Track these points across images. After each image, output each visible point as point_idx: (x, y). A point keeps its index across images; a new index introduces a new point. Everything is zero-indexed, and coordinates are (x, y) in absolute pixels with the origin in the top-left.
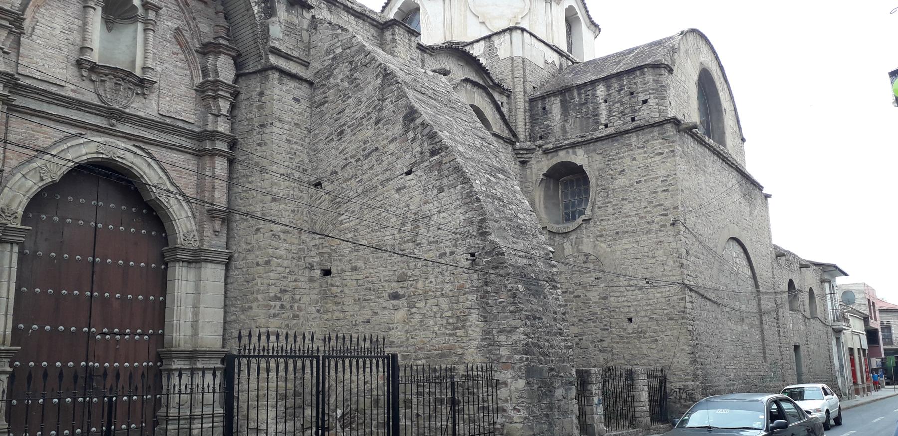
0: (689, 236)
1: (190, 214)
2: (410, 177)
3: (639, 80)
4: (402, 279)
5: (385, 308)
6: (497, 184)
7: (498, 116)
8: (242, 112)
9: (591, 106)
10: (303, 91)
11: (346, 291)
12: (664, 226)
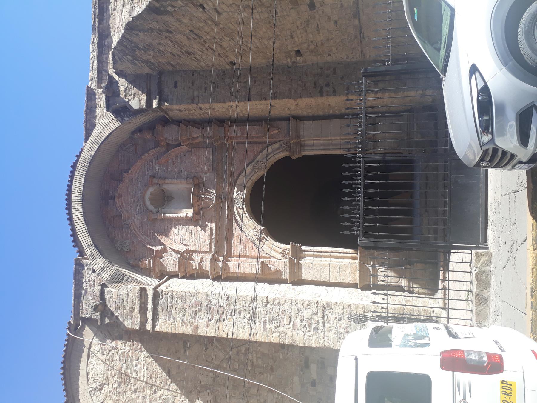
2: (205, 6)
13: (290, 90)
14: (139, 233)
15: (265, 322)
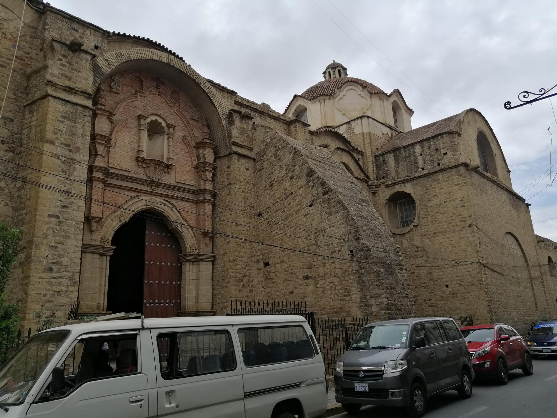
0: (480, 233)
1: (193, 235)
2: (311, 208)
3: (440, 141)
4: (310, 267)
5: (301, 285)
6: (362, 209)
7: (357, 167)
8: (219, 177)
9: (412, 158)
10: (250, 164)
11: (278, 275)
12: (464, 227)
13: (242, 257)
14: (128, 101)
15: (58, 217)
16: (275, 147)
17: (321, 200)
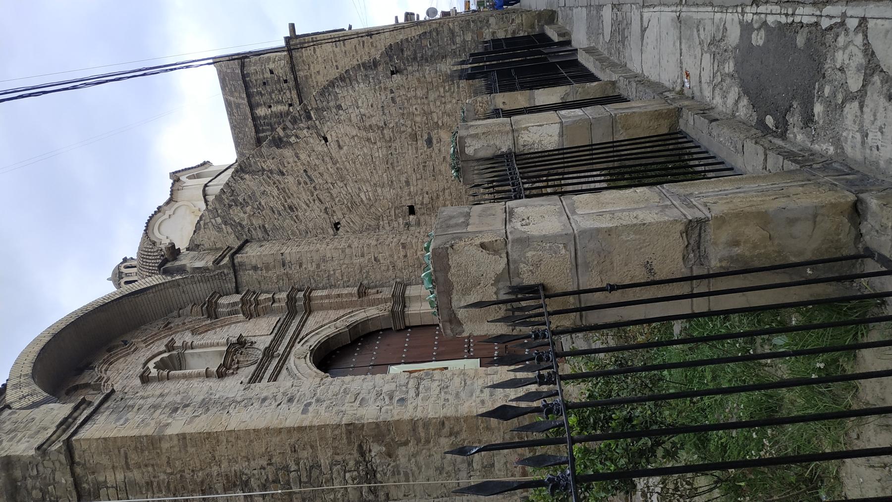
3: (253, 78)
5: (439, 150)
9: (274, 120)
11: (427, 189)
12: (372, 43)
16: (230, 206)
17: (317, 122)
